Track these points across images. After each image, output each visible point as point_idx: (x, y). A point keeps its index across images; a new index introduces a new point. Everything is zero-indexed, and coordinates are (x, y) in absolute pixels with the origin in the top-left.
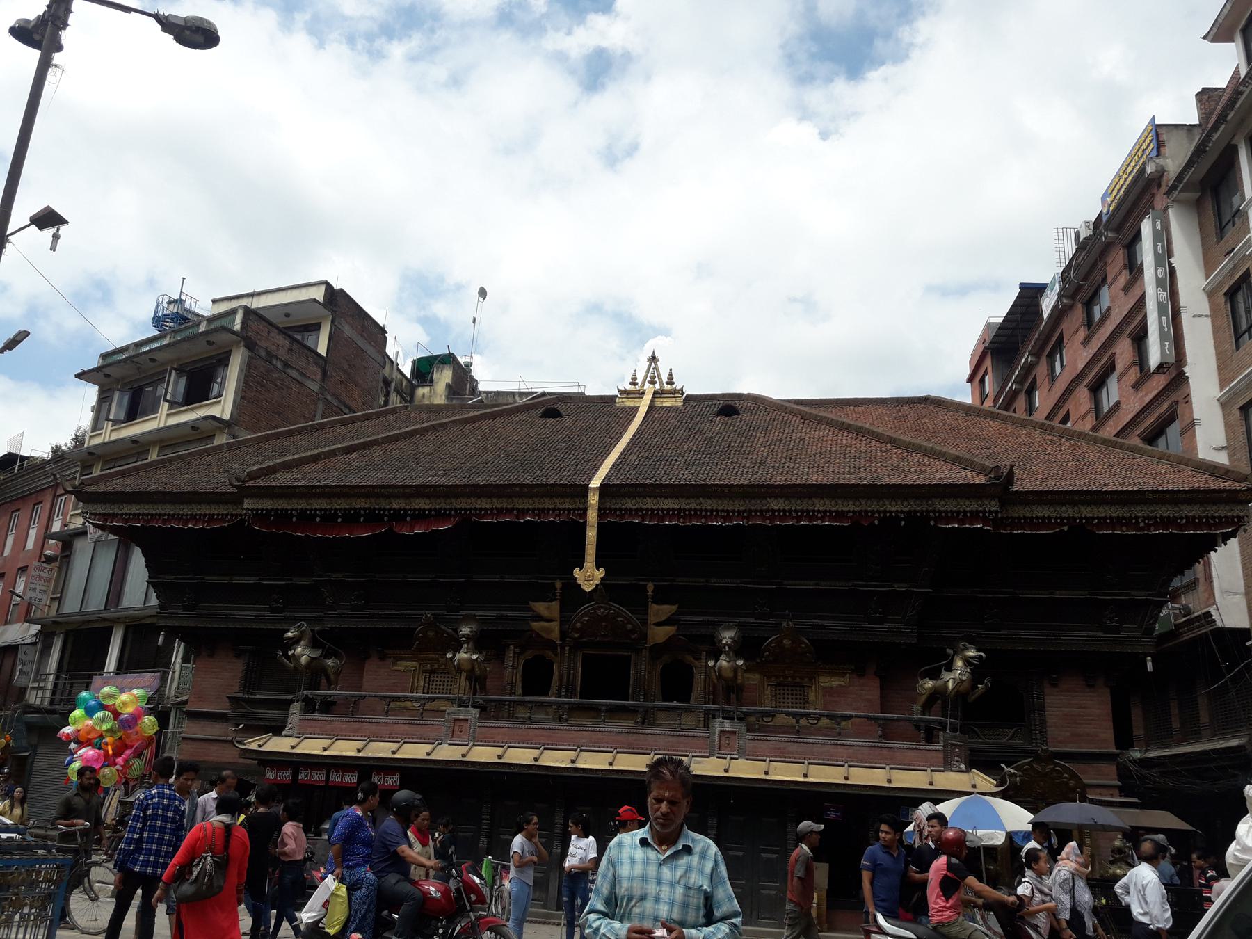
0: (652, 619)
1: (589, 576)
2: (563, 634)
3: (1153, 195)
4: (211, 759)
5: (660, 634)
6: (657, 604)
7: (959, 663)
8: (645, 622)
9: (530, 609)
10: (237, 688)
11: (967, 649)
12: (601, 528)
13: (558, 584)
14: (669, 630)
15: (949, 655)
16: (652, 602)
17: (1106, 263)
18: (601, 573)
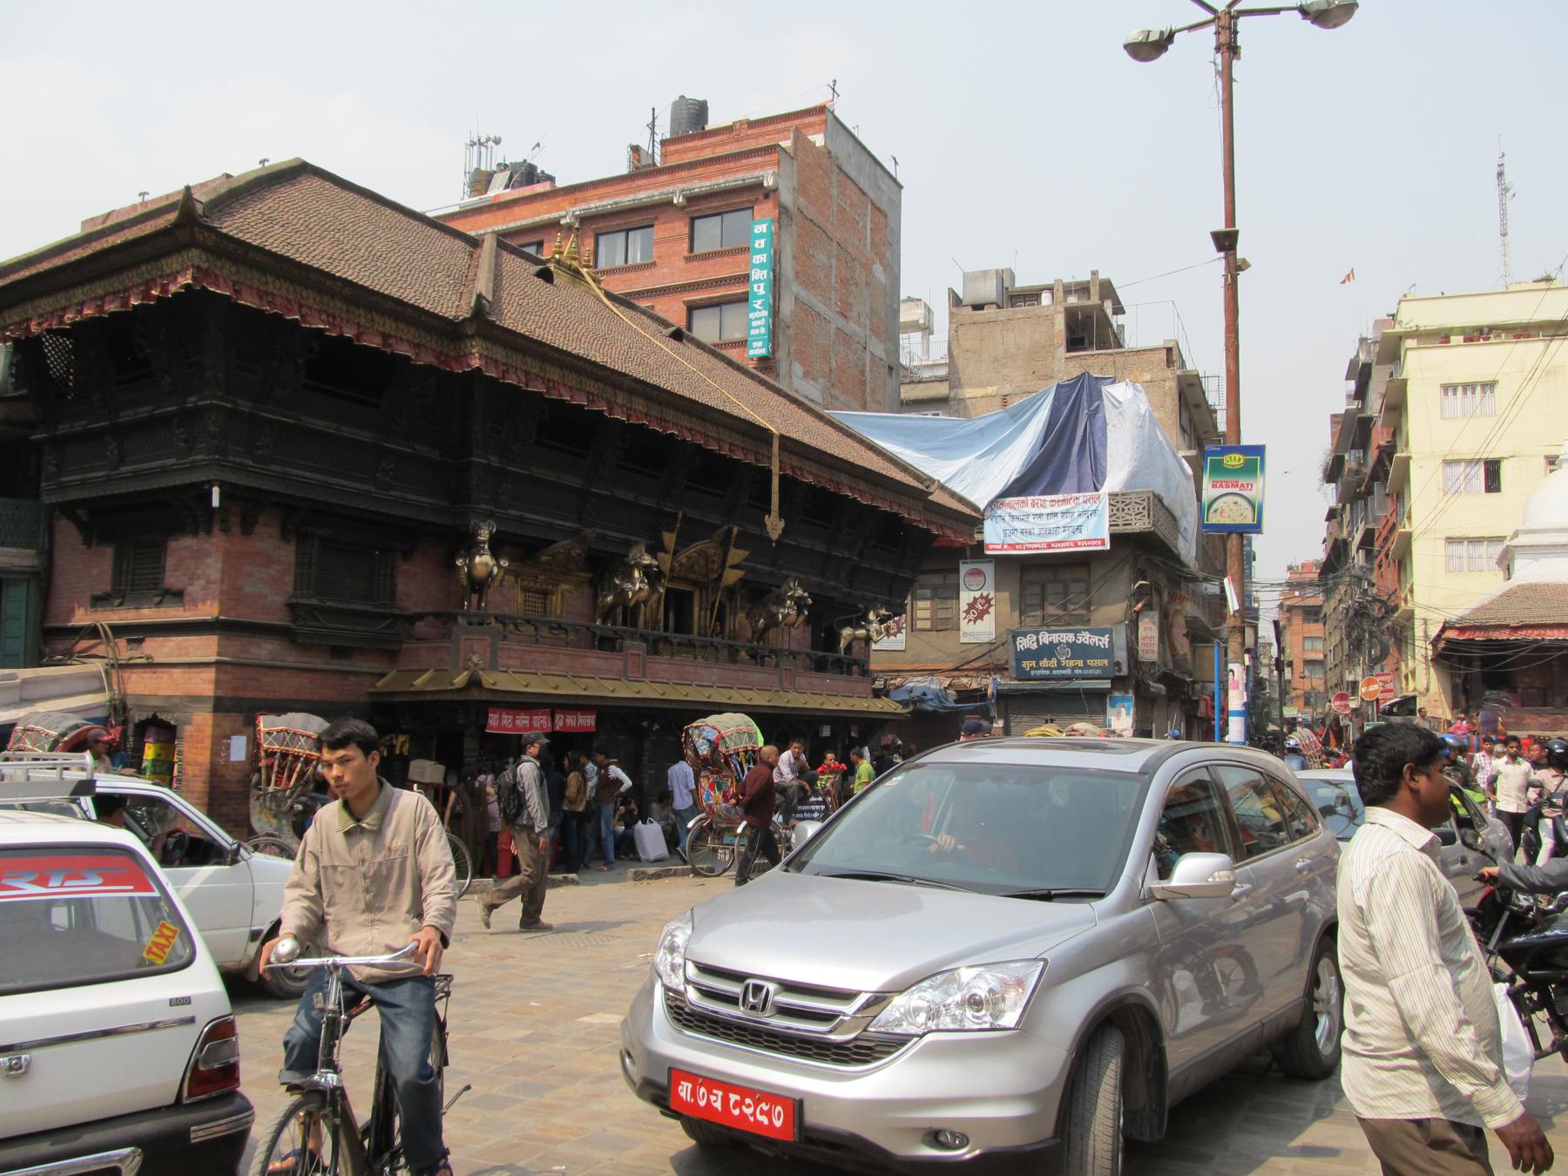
0: (730, 561)
1: (774, 525)
2: (672, 570)
3: (757, 199)
4: (264, 695)
5: (731, 576)
6: (737, 547)
7: (872, 616)
8: (723, 567)
9: (662, 542)
10: (290, 589)
11: (881, 608)
12: (782, 478)
13: (680, 516)
14: (738, 574)
15: (861, 610)
16: (734, 546)
17: (656, 218)
18: (782, 524)
